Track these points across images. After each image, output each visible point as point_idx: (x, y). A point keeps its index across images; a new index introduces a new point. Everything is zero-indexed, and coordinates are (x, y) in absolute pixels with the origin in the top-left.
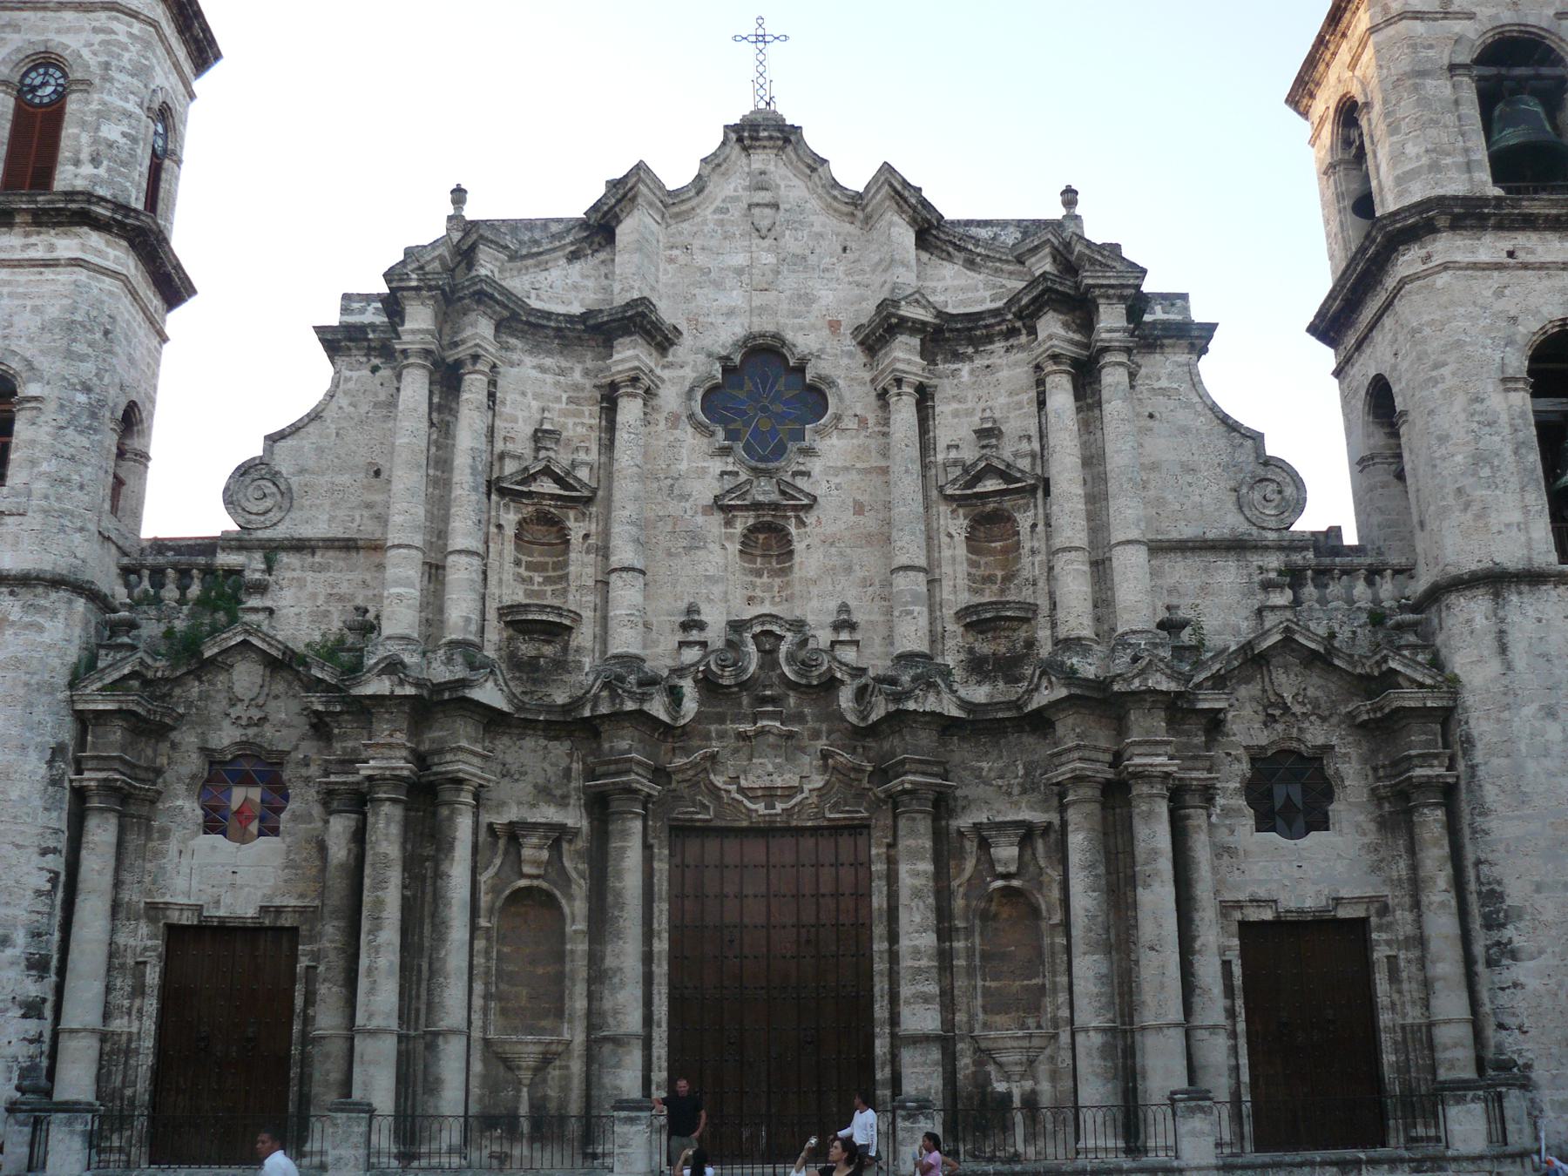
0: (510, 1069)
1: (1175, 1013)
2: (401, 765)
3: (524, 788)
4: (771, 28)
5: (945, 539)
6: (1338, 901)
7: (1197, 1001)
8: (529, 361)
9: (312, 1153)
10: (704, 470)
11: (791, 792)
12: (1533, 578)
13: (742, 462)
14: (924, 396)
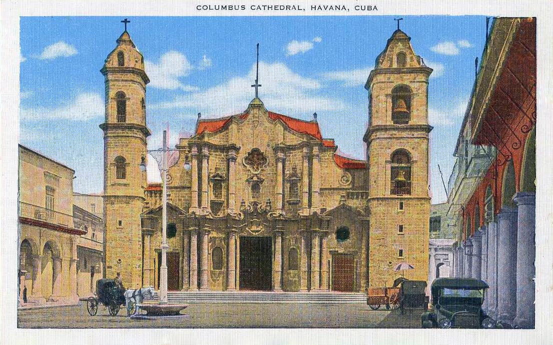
7: (322, 266)
8: (214, 153)
11: (258, 231)
14: (284, 161)
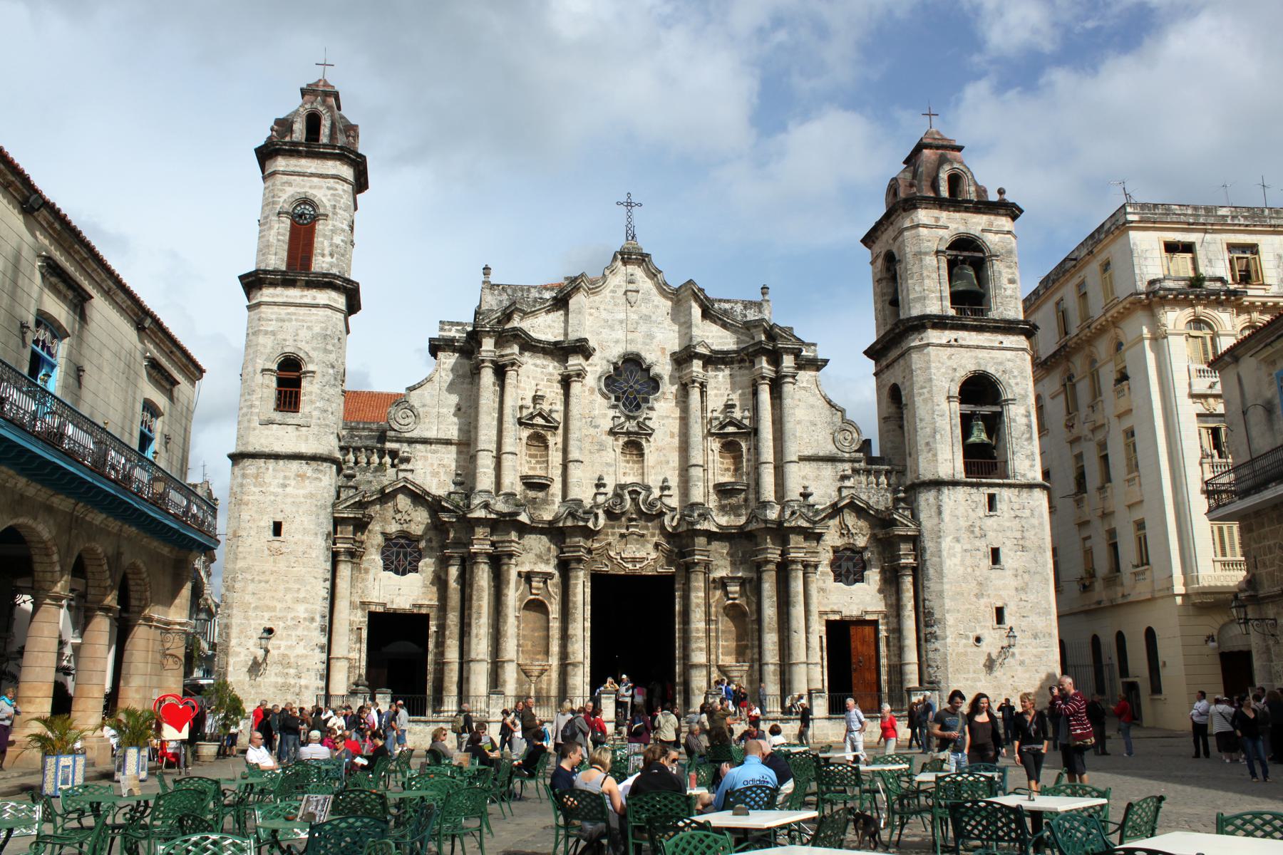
0: (527, 676)
1: (803, 658)
2: (487, 547)
3: (531, 556)
4: (634, 199)
5: (710, 452)
6: (866, 612)
9: (444, 711)
10: (605, 415)
12: (954, 483)
13: (621, 412)
